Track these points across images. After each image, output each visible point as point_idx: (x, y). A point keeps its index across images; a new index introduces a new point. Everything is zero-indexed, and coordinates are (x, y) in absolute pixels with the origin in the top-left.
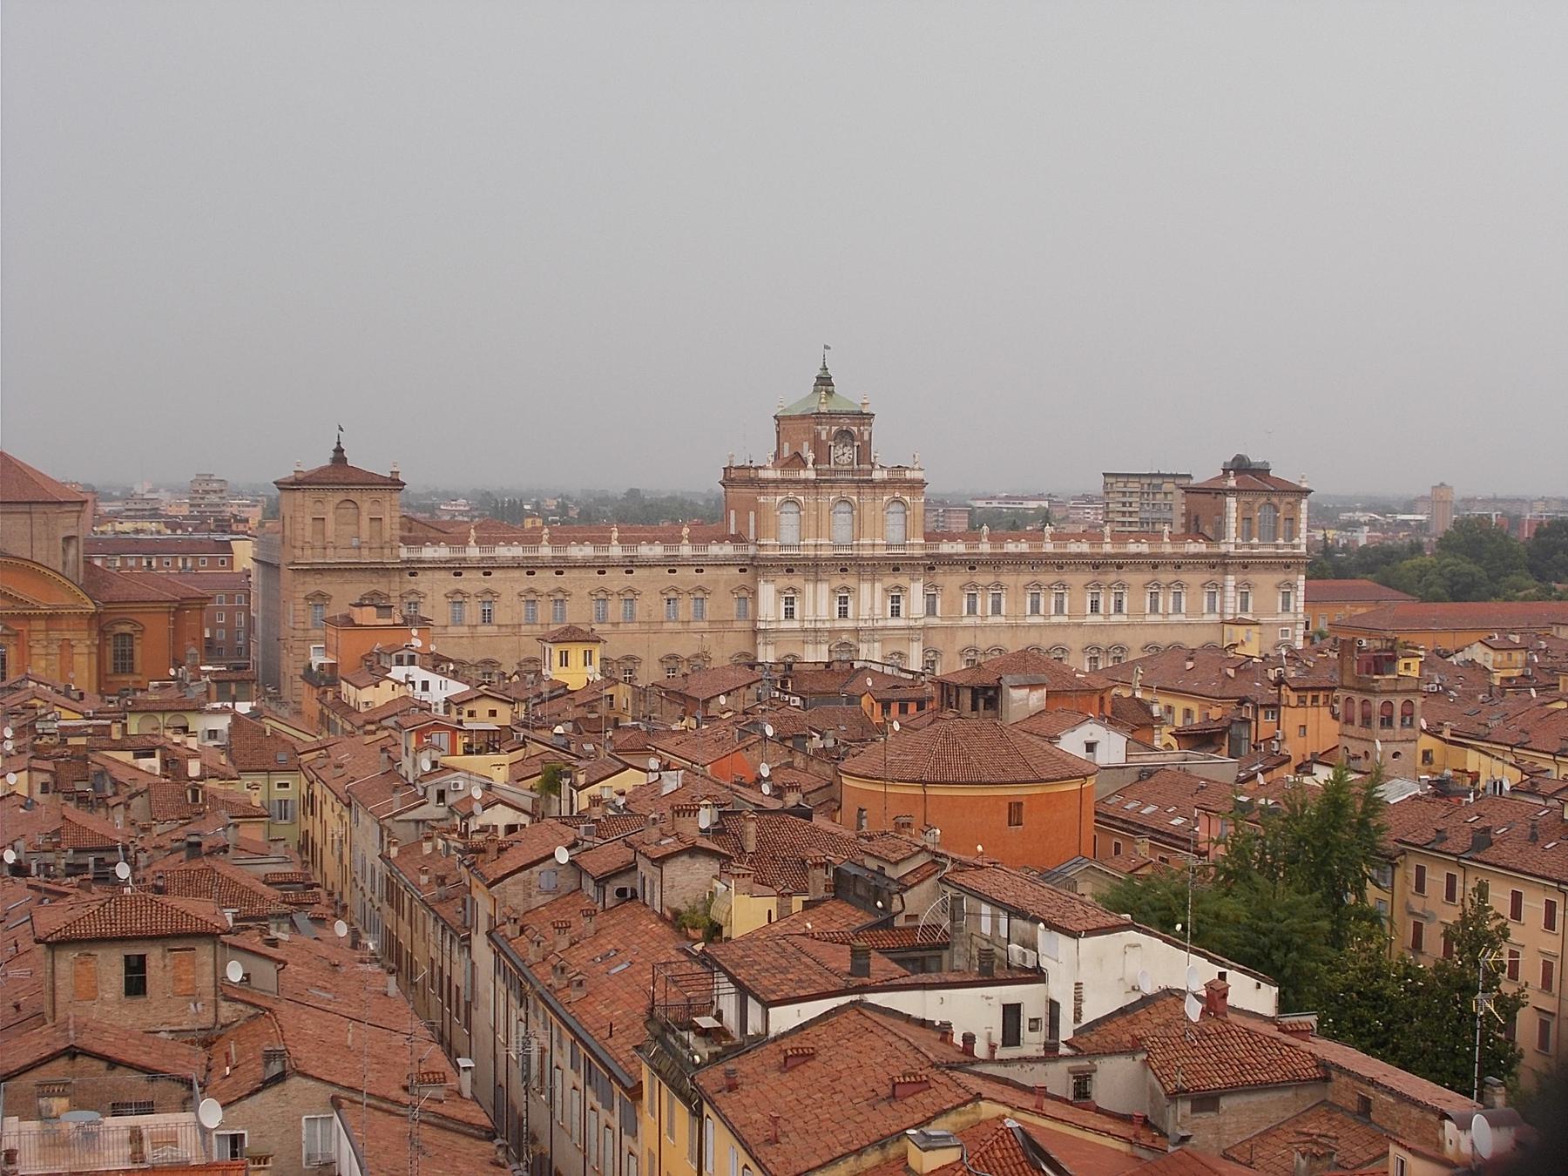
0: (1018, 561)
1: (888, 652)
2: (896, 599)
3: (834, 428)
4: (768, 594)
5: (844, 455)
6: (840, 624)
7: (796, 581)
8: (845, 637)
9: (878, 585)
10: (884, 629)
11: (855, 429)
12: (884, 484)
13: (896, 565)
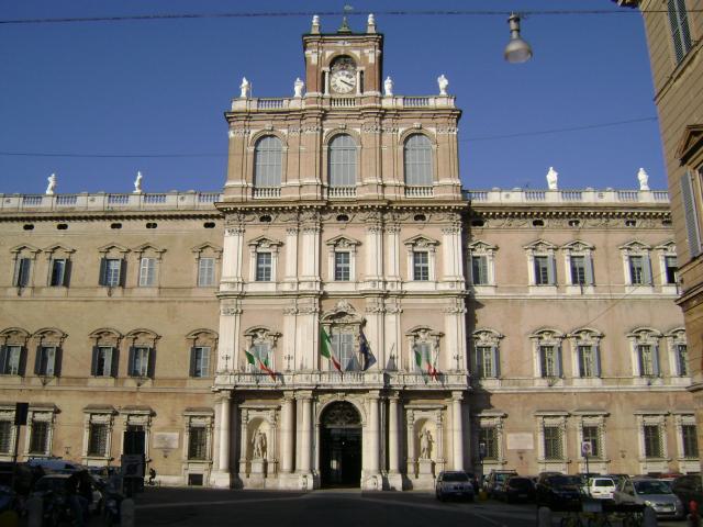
0: (604, 214)
1: (412, 326)
2: (419, 257)
3: (329, 54)
7: (274, 232)
8: (342, 305)
9: (391, 238)
10: (402, 295)
11: (356, 53)
13: (420, 213)
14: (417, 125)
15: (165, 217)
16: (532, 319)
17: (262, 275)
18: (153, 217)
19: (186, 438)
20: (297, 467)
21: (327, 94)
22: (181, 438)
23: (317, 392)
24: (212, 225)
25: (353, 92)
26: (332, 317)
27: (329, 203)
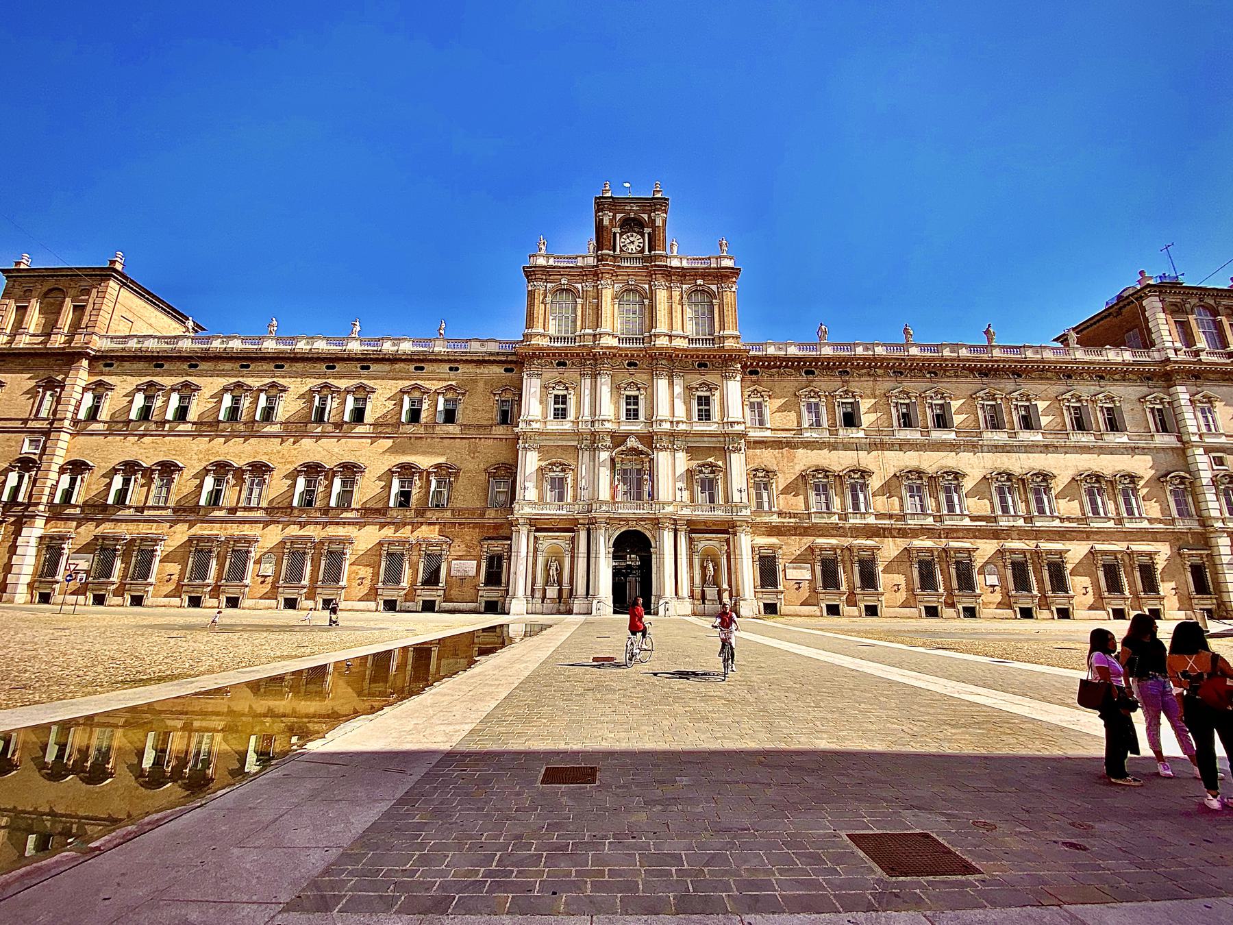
3: (619, 216)
4: (532, 387)
5: (632, 243)
6: (625, 428)
7: (570, 375)
8: (632, 442)
11: (646, 216)
12: (683, 274)
13: (703, 363)
14: (699, 282)
15: (466, 361)
16: (805, 459)
17: (561, 414)
18: (456, 361)
19: (484, 565)
20: (591, 592)
21: (618, 252)
22: (479, 566)
23: (610, 521)
24: (511, 370)
25: (642, 251)
26: (622, 452)
27: (621, 349)
